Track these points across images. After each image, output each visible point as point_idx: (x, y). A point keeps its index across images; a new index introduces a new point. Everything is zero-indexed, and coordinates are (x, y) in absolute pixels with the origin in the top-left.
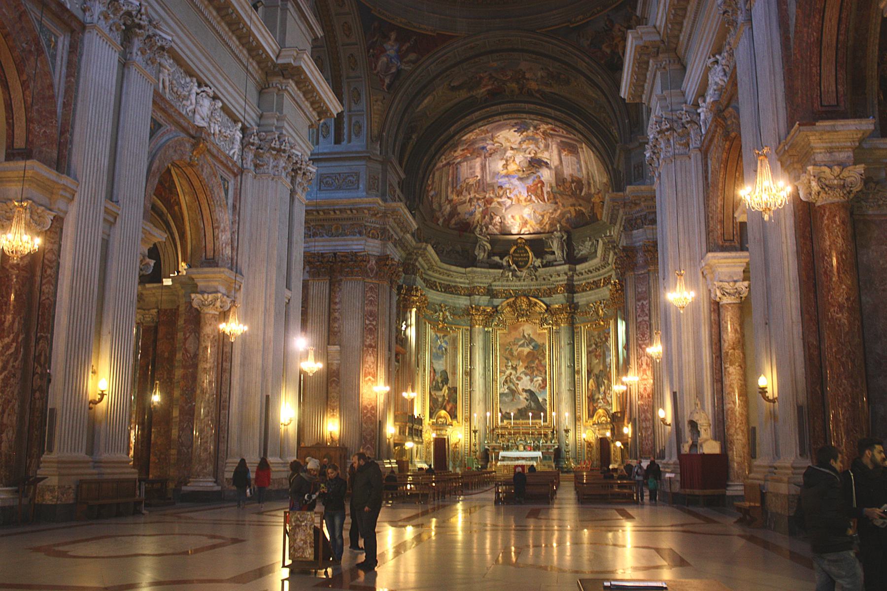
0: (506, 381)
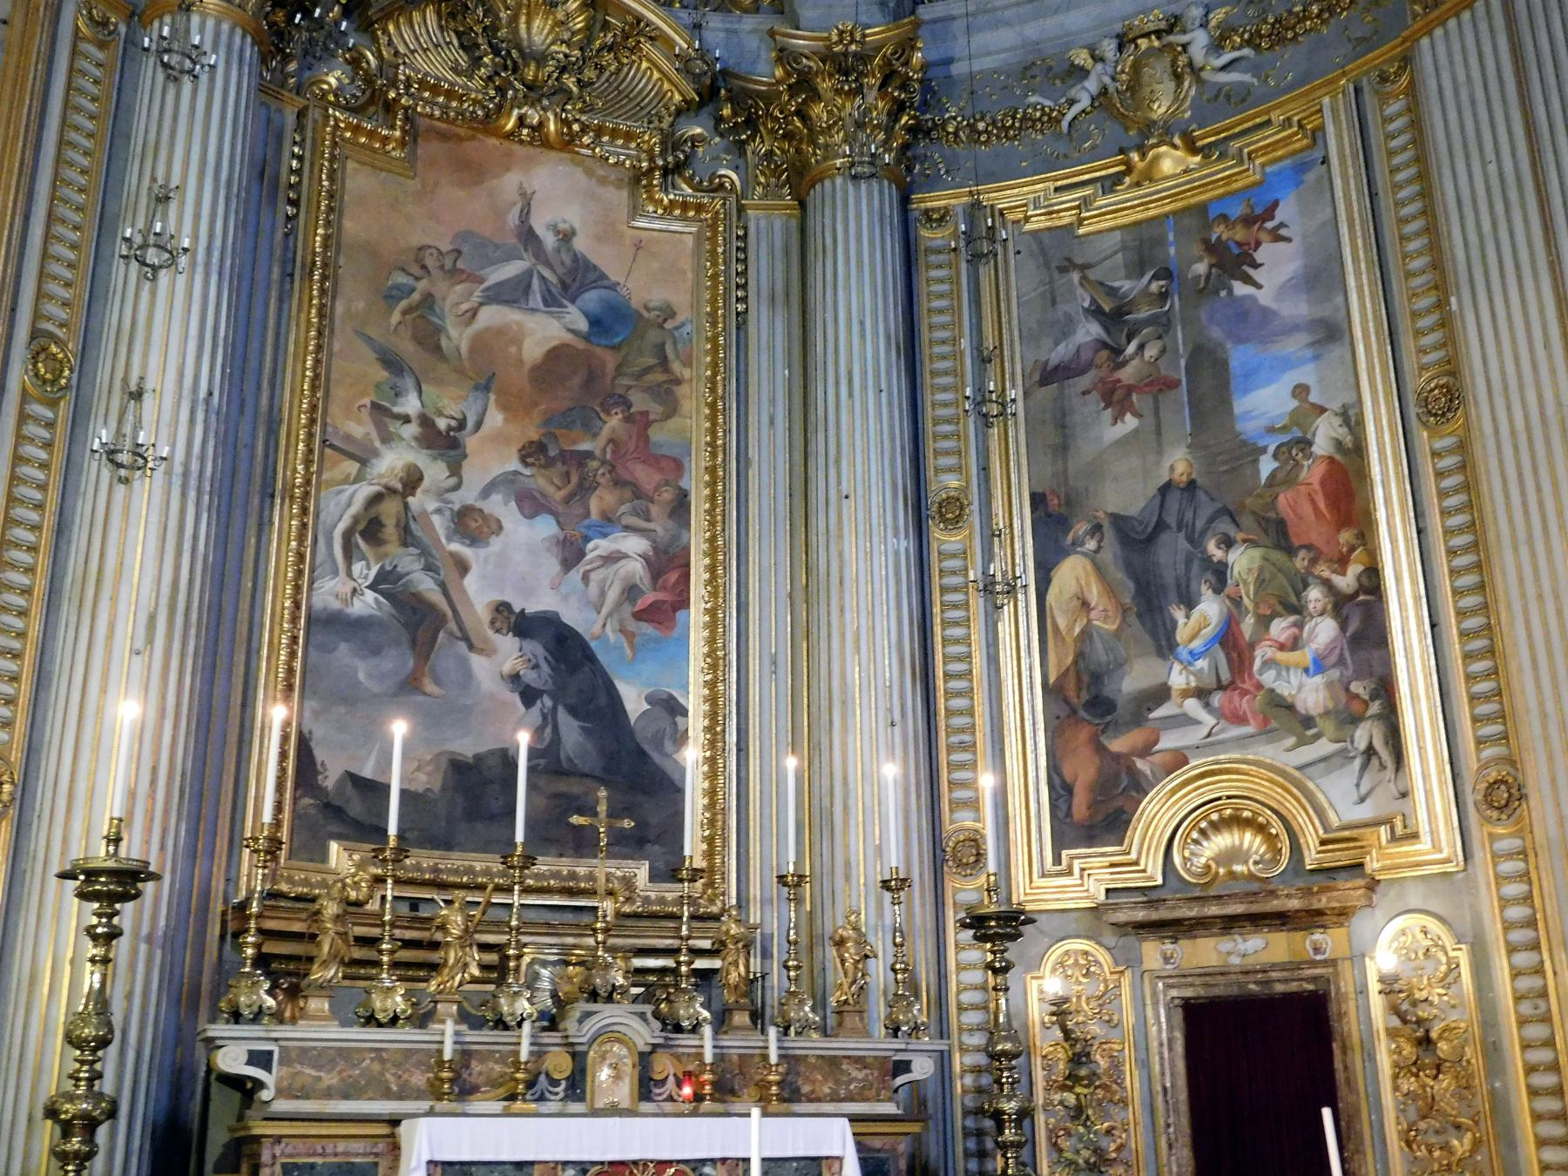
0: (369, 528)
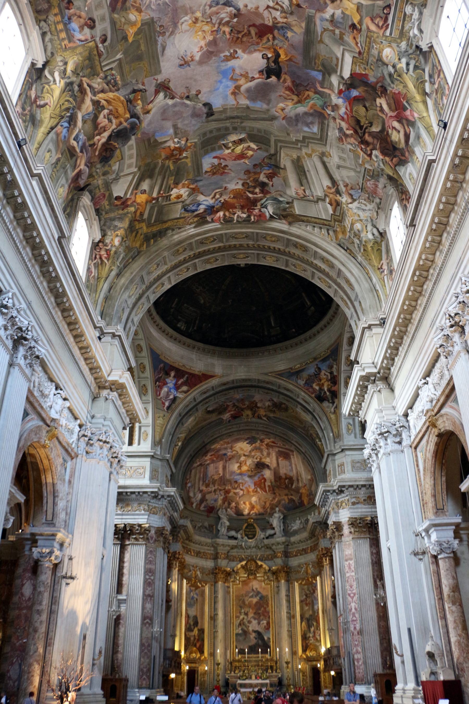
0: (240, 624)
